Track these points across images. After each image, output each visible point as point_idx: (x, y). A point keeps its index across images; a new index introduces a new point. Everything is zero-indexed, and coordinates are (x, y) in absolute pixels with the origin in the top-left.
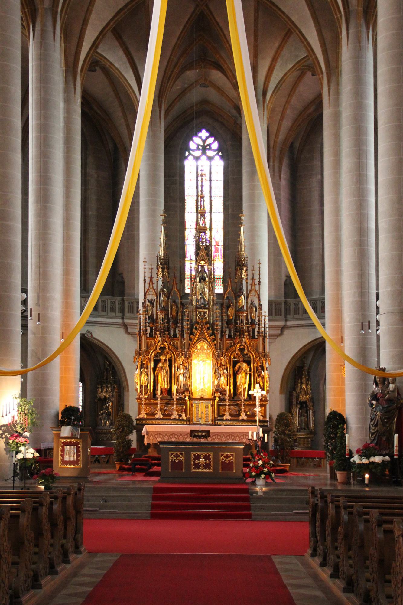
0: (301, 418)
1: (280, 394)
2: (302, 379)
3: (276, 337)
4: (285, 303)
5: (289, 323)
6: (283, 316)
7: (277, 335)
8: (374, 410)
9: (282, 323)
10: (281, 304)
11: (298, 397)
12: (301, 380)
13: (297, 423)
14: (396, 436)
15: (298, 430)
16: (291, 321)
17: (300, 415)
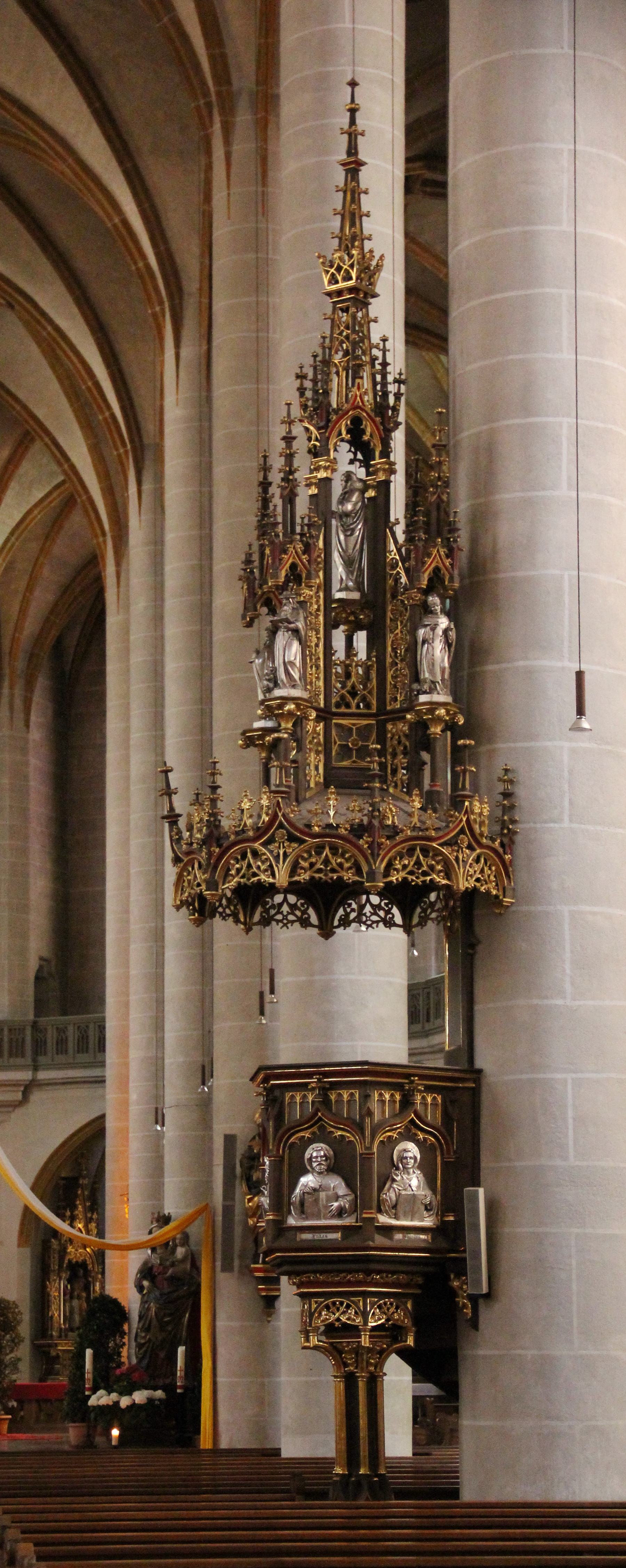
0: (71, 1302)
1: (19, 1246)
2: (74, 1207)
3: (10, 1109)
4: (33, 1027)
5: (42, 1075)
6: (29, 1060)
7: (12, 1103)
8: (145, 1298)
9: (25, 1076)
10: (24, 1029)
11: (63, 1252)
12: (72, 1212)
13: (59, 1316)
14: (181, 1350)
15: (63, 1334)
16: (48, 1069)
17: (68, 1297)
